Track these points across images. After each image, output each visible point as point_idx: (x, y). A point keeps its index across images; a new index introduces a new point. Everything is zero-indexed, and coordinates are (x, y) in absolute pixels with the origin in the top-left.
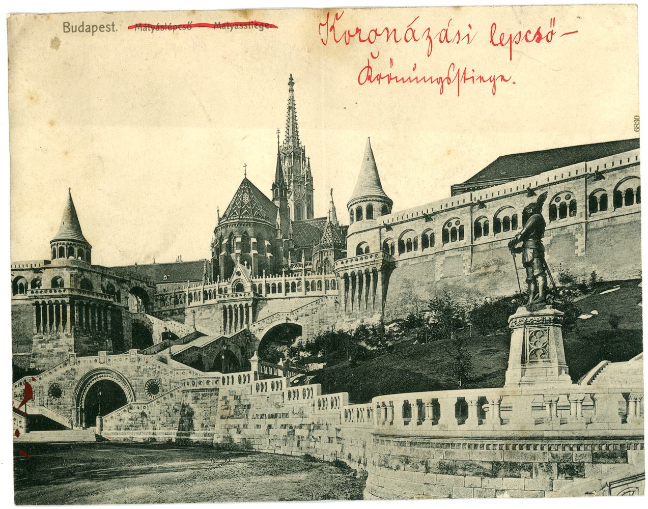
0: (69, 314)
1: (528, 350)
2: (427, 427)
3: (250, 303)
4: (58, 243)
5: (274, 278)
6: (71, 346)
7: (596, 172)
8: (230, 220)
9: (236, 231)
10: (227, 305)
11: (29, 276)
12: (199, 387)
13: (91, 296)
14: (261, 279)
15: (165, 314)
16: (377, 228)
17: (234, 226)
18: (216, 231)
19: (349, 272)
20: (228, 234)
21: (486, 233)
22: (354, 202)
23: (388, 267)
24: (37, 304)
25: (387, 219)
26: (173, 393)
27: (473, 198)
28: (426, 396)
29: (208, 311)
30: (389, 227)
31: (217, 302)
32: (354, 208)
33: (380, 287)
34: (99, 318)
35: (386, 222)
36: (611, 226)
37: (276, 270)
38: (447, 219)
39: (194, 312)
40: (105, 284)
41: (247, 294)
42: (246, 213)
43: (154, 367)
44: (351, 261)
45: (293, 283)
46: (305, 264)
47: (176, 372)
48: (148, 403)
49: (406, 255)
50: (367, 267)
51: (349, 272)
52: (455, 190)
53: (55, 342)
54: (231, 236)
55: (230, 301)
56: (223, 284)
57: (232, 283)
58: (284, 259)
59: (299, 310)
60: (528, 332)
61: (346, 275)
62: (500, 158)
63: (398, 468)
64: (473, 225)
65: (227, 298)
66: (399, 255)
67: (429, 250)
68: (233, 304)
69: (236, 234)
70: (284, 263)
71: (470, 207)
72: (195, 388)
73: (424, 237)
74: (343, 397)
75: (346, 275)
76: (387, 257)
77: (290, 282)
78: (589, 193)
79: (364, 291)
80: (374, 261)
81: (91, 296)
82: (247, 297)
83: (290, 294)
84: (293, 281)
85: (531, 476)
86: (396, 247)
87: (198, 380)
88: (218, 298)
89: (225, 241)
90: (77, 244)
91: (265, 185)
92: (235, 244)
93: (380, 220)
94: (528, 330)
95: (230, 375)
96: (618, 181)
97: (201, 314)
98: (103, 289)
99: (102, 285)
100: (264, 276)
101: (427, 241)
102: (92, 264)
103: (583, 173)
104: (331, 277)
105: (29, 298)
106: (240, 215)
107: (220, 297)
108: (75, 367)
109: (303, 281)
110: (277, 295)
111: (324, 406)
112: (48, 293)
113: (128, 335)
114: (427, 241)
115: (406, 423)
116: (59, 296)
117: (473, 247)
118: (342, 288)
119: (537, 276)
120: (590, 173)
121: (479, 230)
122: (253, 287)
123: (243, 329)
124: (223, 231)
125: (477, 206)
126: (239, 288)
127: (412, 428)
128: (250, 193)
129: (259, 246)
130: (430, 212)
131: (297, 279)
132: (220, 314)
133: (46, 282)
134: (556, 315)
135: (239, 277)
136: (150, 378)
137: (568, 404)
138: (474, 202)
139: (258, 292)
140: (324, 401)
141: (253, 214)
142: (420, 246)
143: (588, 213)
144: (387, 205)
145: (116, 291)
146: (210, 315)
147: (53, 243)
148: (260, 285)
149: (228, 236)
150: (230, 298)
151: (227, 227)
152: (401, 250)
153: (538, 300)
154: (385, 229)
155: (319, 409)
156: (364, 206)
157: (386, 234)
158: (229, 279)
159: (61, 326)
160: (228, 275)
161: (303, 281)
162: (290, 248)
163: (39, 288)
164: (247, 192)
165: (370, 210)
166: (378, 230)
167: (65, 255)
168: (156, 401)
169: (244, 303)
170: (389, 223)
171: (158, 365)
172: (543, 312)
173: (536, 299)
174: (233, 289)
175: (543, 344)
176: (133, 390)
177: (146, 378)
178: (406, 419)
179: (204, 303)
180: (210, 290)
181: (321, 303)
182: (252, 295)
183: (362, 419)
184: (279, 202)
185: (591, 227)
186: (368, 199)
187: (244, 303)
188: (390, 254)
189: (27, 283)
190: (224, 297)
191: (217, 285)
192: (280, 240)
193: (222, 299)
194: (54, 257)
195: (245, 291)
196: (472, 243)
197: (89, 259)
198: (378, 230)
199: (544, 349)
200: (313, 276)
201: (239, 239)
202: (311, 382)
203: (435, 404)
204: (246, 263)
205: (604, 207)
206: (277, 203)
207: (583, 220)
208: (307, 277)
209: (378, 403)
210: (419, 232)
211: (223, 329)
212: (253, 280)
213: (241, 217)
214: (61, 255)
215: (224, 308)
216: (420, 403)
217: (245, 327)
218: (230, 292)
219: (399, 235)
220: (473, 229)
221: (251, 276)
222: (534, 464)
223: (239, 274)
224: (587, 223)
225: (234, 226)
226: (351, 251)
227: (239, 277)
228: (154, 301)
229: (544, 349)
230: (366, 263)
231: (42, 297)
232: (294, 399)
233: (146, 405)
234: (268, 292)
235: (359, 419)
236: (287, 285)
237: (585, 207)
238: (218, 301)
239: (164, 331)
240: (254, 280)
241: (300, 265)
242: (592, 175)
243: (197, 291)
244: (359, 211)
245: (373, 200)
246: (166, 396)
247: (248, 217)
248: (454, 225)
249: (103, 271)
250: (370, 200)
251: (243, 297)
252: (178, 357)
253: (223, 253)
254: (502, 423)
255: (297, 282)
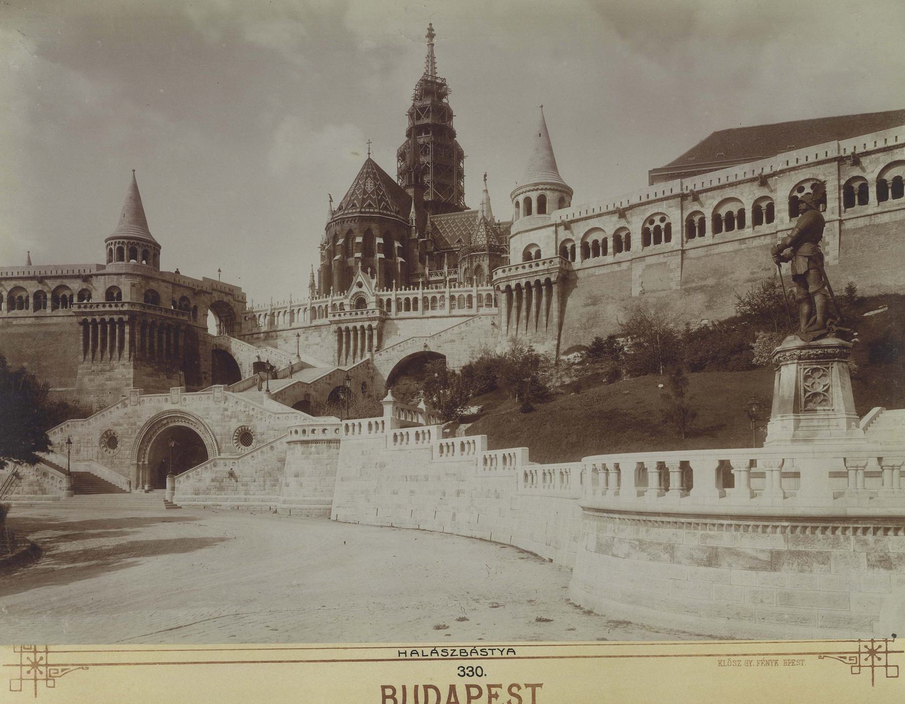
0: (127, 337)
1: (802, 394)
2: (673, 501)
3: (375, 324)
4: (116, 242)
5: (408, 291)
6: (129, 379)
7: (853, 153)
8: (348, 213)
9: (355, 229)
10: (343, 326)
11: (76, 286)
12: (311, 437)
13: (158, 313)
14: (389, 292)
15: (258, 338)
16: (552, 225)
17: (353, 222)
18: (328, 228)
19: (513, 284)
20: (345, 232)
21: (702, 233)
22: (521, 191)
23: (567, 280)
24: (84, 323)
25: (565, 214)
26: (274, 445)
27: (684, 187)
28: (673, 458)
29: (316, 334)
30: (567, 225)
31: (329, 323)
32: (521, 199)
33: (555, 305)
34: (168, 342)
35: (564, 218)
36: (874, 225)
37: (409, 279)
38: (648, 214)
39: (298, 336)
40: (177, 297)
41: (371, 311)
42: (370, 206)
43: (247, 409)
44: (517, 269)
45: (434, 299)
46: (448, 273)
47: (277, 416)
48: (239, 458)
49: (591, 261)
50: (538, 278)
51: (513, 284)
52: (657, 176)
53: (108, 374)
54: (349, 235)
55: (348, 321)
56: (336, 298)
57: (350, 297)
58: (420, 265)
59: (442, 334)
60: (802, 370)
61: (508, 287)
62: (717, 135)
63: (628, 555)
64: (684, 223)
65: (343, 317)
66: (582, 262)
67: (623, 255)
68: (351, 326)
69: (356, 231)
70: (419, 271)
71: (680, 198)
72: (305, 438)
73: (617, 238)
74: (520, 453)
75: (508, 287)
76: (565, 264)
77: (430, 297)
78: (843, 182)
79: (534, 309)
80: (548, 270)
81: (158, 313)
82: (371, 315)
83: (430, 313)
84: (433, 295)
85: (829, 571)
86: (578, 251)
87: (311, 428)
88: (330, 318)
89: (341, 241)
90: (141, 243)
91: (391, 167)
92: (354, 245)
93: (556, 215)
94: (802, 366)
95: (356, 422)
96: (881, 167)
97: (307, 338)
98: (174, 303)
99: (173, 298)
100: (421, 286)
101: (621, 243)
102: (160, 270)
103: (835, 155)
104: (485, 289)
105: (74, 314)
106: (362, 207)
107: (334, 316)
108: (138, 407)
109: (447, 295)
110: (412, 313)
111: (491, 465)
112: (101, 309)
113: (206, 365)
114: (621, 243)
115: (640, 494)
116: (116, 313)
117: (683, 251)
118: (503, 303)
119: (815, 293)
120: (843, 155)
121: (693, 228)
122: (380, 302)
123: (364, 360)
124: (338, 228)
125: (690, 198)
126: (361, 303)
127: (652, 500)
128: (375, 178)
129: (387, 248)
130: (625, 205)
131: (439, 293)
132: (332, 340)
133: (98, 295)
134: (841, 347)
135: (361, 290)
136: (240, 424)
137: (844, 470)
138: (685, 192)
139: (385, 310)
140: (492, 459)
141: (379, 207)
142: (610, 250)
143: (843, 208)
144: (564, 196)
145: (192, 306)
146: (318, 340)
147: (110, 242)
148: (389, 301)
149: (344, 235)
150: (348, 317)
151: (343, 223)
152: (586, 255)
153: (815, 326)
154: (562, 228)
155: (485, 469)
156: (534, 196)
157: (563, 234)
158: (346, 291)
159: (116, 353)
160: (344, 287)
161: (447, 295)
162: (428, 250)
163: (88, 301)
164: (371, 178)
165: (542, 201)
166: (553, 228)
167: (125, 257)
168: (249, 456)
169: (366, 324)
170: (569, 219)
171: (252, 407)
172: (825, 342)
173: (811, 325)
174: (351, 305)
175: (824, 386)
176: (216, 440)
177: (234, 425)
178: (641, 489)
179: (311, 323)
180: (320, 306)
181: (472, 325)
182: (377, 313)
183: (552, 485)
184: (413, 190)
185: (848, 225)
186: (540, 187)
187: (366, 324)
188: (569, 259)
189: (72, 296)
190: (340, 315)
191: (329, 299)
192: (416, 240)
193: (337, 318)
194: (110, 261)
195: (368, 308)
196: (682, 246)
197: (156, 264)
198: (553, 228)
199: (826, 394)
200: (461, 289)
201: (359, 239)
202: (468, 432)
203: (685, 467)
204: (369, 270)
205: (864, 201)
206: (410, 192)
207: (837, 217)
208: (453, 289)
209: (594, 465)
210: (610, 231)
211: (337, 358)
212: (378, 293)
213: (363, 210)
214: (121, 258)
215: (339, 332)
216: (661, 466)
217: (368, 356)
218: (347, 308)
219: (581, 235)
220: (684, 228)
221: (377, 288)
222: (832, 553)
223: (360, 285)
224: (841, 222)
225: (353, 222)
226: (515, 256)
227: (361, 290)
228: (243, 320)
229: (826, 394)
230: (536, 272)
231: (92, 314)
232: (447, 456)
233: (236, 461)
234: (399, 309)
235: (547, 484)
236: (479, 297)
237: (837, 200)
238: (330, 321)
239: (256, 360)
240: (381, 293)
241: (441, 274)
242: (848, 157)
243: (301, 307)
244: (528, 201)
245: (546, 189)
246: (264, 449)
247: (372, 210)
248: (657, 222)
249: (175, 281)
250: (542, 189)
251: (365, 316)
252: (278, 397)
253: (337, 257)
254: (753, 495)
255: (438, 296)
